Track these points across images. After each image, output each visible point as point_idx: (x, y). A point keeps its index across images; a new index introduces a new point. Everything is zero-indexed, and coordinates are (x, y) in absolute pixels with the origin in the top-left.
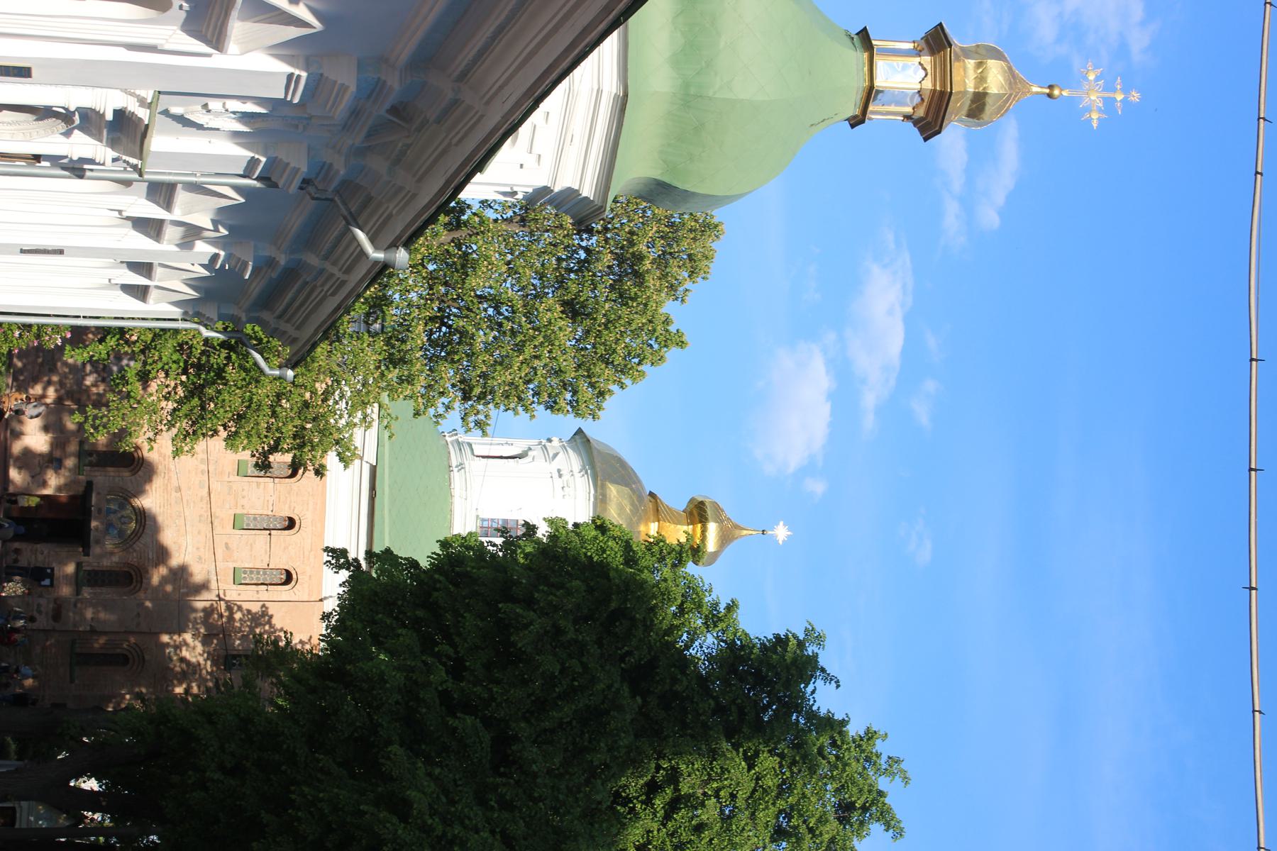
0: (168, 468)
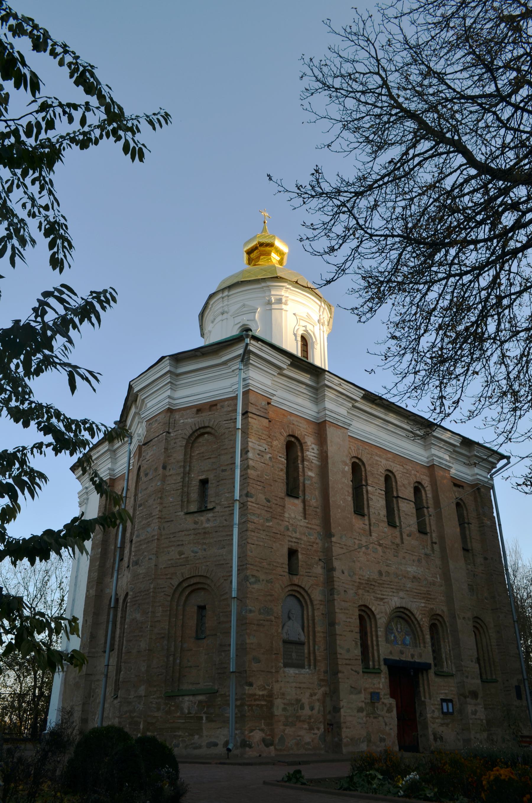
0: (367, 581)
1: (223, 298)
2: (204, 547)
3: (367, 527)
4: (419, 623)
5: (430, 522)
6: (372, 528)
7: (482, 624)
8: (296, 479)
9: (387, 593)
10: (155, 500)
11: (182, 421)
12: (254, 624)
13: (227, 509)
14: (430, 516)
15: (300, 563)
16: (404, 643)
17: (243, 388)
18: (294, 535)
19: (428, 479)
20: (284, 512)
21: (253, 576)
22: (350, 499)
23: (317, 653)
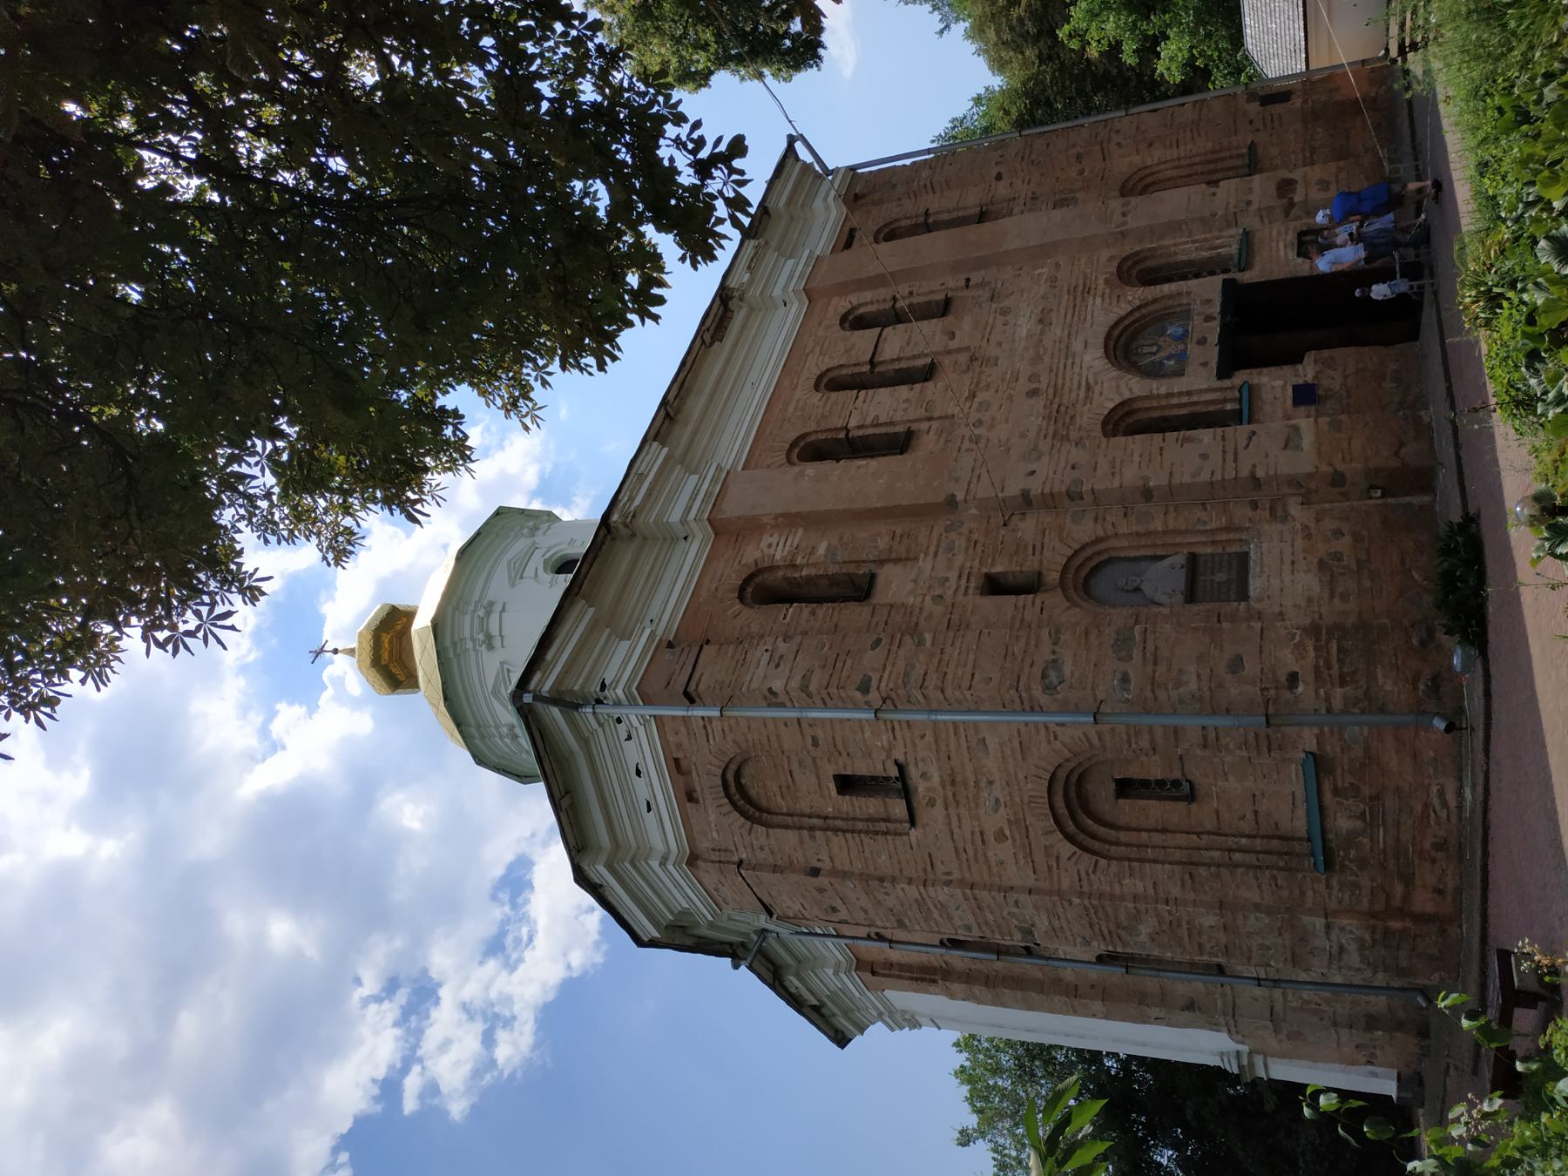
0: (1049, 420)
1: (483, 737)
2: (983, 784)
3: (935, 425)
4: (1139, 308)
5: (924, 294)
6: (936, 415)
7: (1136, 178)
8: (833, 580)
9: (1076, 378)
10: (887, 894)
11: (715, 834)
12: (1154, 672)
13: (898, 732)
14: (911, 293)
15: (1015, 568)
16: (1183, 338)
17: (636, 704)
18: (953, 583)
19: (835, 301)
20: (903, 604)
21: (1044, 676)
22: (873, 464)
23: (1213, 525)
